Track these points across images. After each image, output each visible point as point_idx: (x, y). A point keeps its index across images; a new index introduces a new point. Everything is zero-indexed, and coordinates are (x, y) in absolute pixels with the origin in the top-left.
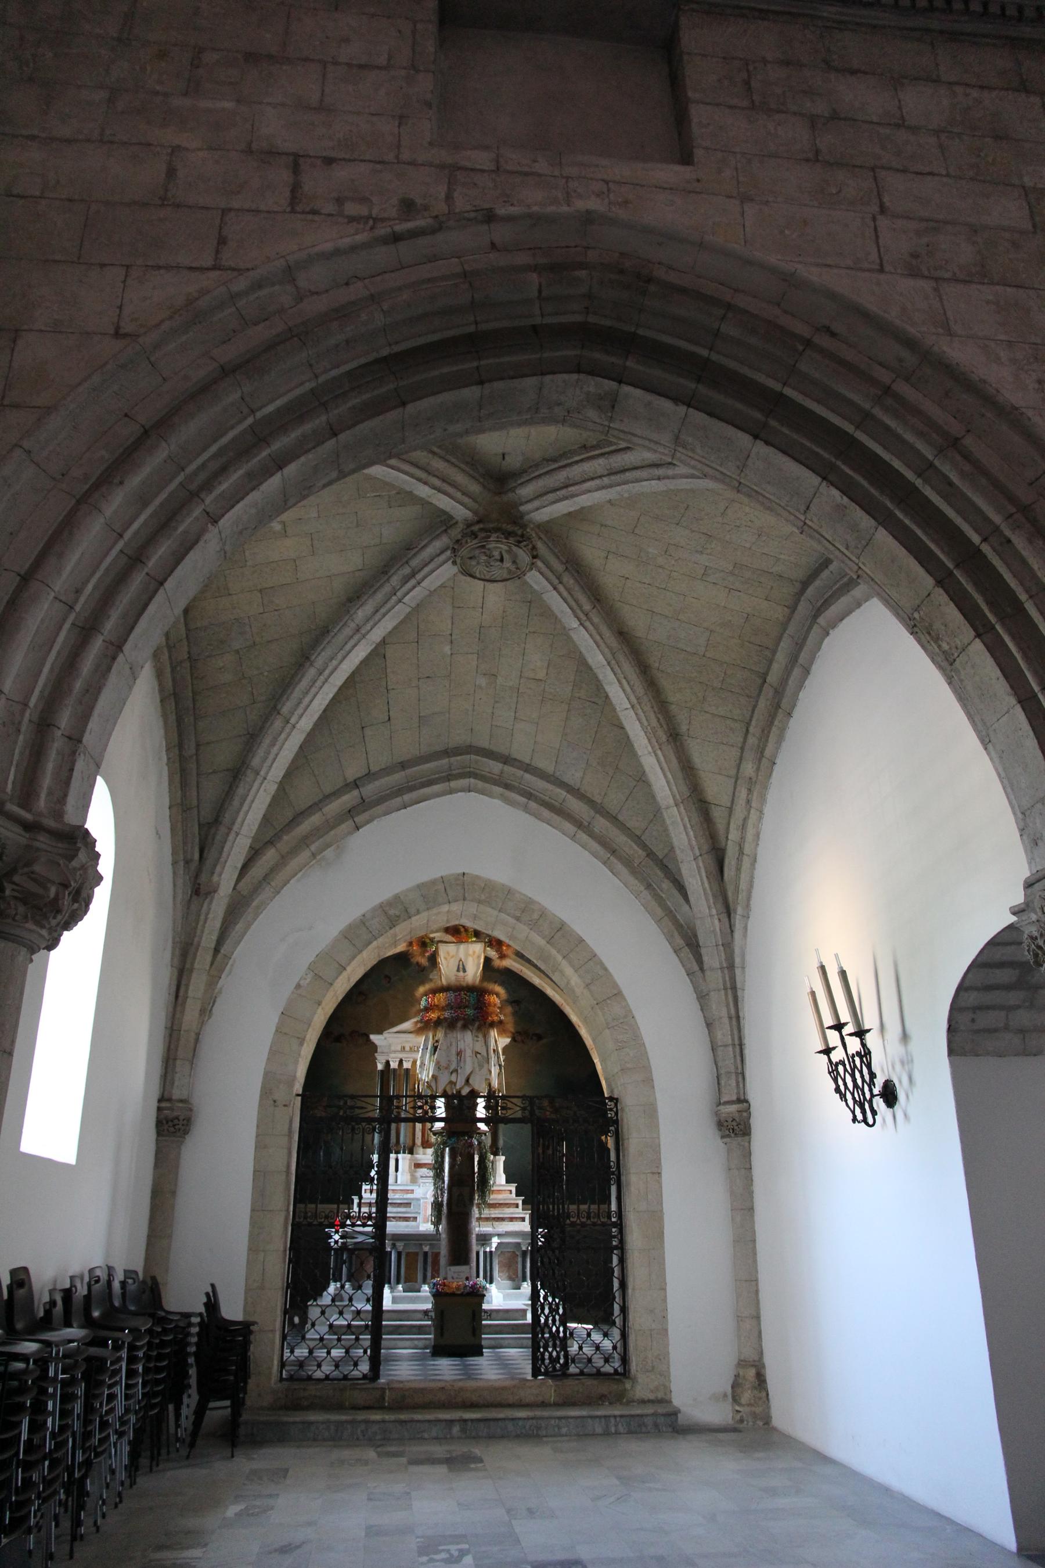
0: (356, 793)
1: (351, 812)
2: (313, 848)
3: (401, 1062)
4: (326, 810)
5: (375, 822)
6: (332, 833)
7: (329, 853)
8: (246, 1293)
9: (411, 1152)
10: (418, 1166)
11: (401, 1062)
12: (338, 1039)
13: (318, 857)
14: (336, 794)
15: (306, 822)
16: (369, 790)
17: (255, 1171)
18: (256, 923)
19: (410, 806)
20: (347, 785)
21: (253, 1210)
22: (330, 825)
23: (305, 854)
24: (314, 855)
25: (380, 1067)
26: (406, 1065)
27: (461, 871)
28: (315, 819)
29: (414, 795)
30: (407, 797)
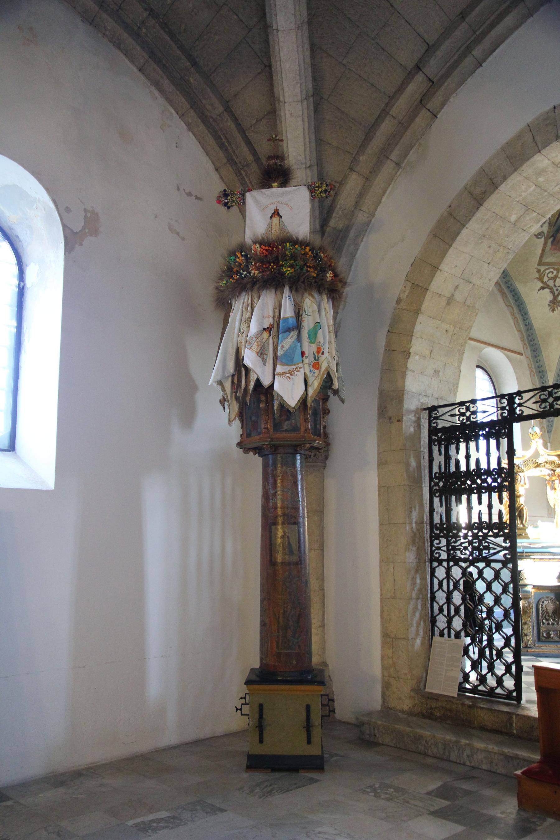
0: (420, 77)
1: (422, 102)
2: (394, 156)
4: (393, 111)
5: (452, 100)
6: (409, 132)
7: (412, 156)
8: (381, 602)
13: (403, 165)
14: (401, 89)
15: (378, 134)
16: (433, 67)
17: (380, 487)
18: (359, 252)
19: (484, 60)
20: (409, 73)
21: (381, 524)
22: (404, 125)
23: (388, 166)
24: (398, 165)
27: (552, 106)
28: (386, 127)
29: (487, 43)
30: (477, 52)
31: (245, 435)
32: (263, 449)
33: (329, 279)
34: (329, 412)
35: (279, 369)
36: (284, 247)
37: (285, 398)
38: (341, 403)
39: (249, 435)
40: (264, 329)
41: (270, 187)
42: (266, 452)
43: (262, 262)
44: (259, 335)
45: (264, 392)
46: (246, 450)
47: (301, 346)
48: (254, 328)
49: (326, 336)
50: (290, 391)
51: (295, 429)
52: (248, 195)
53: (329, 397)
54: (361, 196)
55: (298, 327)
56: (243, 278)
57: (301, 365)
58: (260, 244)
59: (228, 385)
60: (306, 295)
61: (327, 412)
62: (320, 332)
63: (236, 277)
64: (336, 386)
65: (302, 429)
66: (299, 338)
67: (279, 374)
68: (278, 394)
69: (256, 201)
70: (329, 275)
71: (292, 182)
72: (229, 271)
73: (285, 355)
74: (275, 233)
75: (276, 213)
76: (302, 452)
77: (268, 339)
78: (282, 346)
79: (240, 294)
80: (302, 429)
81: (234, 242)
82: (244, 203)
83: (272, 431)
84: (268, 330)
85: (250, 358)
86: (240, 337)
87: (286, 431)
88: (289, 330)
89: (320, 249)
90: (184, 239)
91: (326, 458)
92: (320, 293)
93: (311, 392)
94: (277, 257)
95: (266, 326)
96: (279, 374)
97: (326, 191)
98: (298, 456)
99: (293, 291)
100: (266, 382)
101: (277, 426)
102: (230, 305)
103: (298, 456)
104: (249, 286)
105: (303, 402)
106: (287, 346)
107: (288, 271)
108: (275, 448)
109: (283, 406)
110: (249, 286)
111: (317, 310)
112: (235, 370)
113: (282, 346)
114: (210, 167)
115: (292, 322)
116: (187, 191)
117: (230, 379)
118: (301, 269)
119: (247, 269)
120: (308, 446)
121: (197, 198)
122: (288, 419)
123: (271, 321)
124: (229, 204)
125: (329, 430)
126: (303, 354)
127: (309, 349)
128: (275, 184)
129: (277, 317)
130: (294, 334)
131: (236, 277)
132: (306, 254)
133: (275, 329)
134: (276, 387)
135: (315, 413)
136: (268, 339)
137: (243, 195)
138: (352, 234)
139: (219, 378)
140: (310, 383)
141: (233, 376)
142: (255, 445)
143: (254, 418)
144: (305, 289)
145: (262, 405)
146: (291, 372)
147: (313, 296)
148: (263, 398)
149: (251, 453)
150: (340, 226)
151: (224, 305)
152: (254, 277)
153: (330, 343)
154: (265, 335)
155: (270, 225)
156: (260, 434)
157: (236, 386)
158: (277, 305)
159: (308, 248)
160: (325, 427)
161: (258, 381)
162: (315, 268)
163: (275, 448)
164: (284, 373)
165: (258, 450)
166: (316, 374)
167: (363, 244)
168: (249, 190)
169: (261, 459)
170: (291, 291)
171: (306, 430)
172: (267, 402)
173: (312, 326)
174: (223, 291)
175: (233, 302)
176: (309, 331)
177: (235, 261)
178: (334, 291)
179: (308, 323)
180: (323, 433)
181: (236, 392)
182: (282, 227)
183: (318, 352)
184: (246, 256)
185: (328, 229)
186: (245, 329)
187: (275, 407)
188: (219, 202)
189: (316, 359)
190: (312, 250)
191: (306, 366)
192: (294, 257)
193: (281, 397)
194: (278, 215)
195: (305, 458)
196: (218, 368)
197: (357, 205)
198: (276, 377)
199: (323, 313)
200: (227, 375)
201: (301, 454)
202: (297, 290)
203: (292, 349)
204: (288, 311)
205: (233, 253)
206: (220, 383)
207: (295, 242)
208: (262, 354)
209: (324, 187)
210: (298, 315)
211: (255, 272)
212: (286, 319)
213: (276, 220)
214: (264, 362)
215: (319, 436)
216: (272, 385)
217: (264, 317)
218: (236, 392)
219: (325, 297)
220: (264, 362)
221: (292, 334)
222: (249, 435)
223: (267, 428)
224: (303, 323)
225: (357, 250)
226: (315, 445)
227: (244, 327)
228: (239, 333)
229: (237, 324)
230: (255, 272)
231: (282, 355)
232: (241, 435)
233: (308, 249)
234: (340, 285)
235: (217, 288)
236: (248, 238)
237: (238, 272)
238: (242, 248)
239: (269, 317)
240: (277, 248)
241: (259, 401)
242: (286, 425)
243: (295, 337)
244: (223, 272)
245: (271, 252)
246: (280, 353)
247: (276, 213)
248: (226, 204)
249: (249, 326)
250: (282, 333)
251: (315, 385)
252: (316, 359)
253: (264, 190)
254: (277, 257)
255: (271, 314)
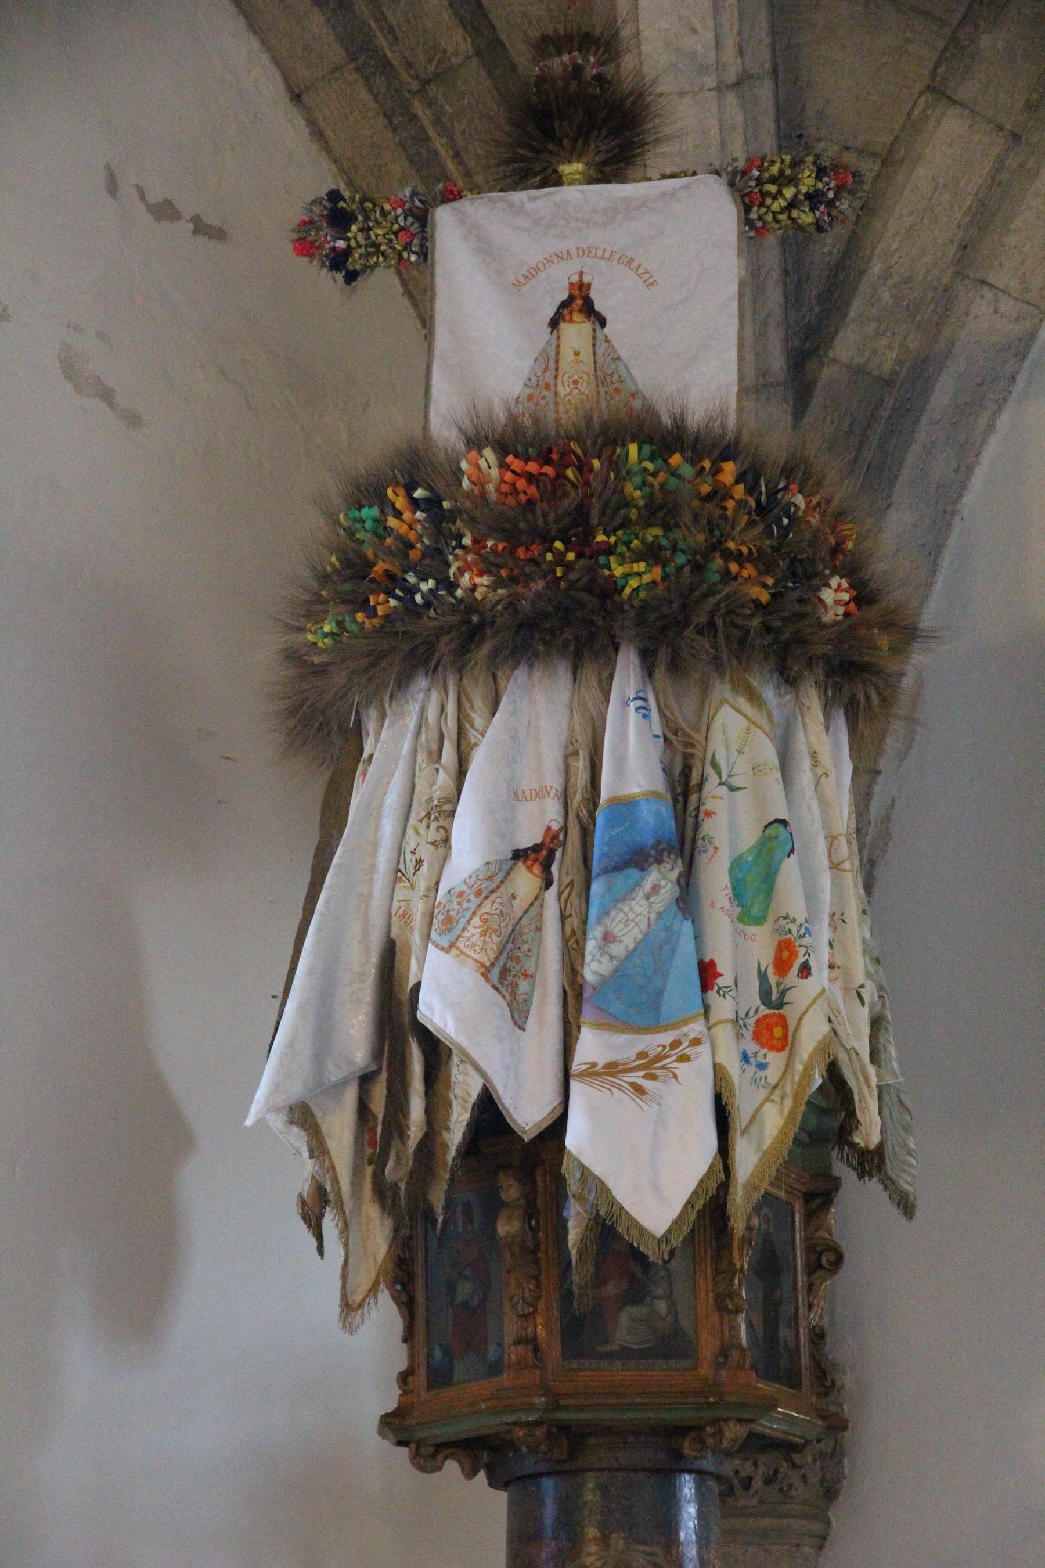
18: (978, 481)
31: (422, 1376)
32: (512, 1445)
33: (833, 614)
34: (838, 1260)
35: (591, 1046)
36: (615, 464)
37: (623, 1193)
38: (896, 1213)
39: (440, 1377)
40: (518, 855)
41: (553, 180)
42: (530, 1465)
43: (511, 535)
44: (493, 881)
45: (515, 1160)
46: (428, 1454)
47: (698, 938)
48: (470, 849)
49: (817, 888)
50: (644, 1156)
51: (672, 1345)
52: (444, 216)
53: (836, 1183)
54: (986, 217)
55: (684, 844)
56: (413, 611)
57: (696, 1028)
58: (503, 448)
59: (340, 1126)
60: (722, 689)
61: (826, 1259)
62: (790, 870)
63: (386, 604)
64: (870, 1131)
65: (708, 1346)
66: (687, 898)
67: (591, 1073)
68: (585, 1173)
69: (487, 251)
70: (834, 596)
71: (657, 158)
72: (352, 577)
73: (618, 978)
74: (573, 396)
75: (579, 303)
76: (708, 1464)
77: (538, 898)
78: (608, 938)
79: (403, 682)
80: (708, 1346)
81: (380, 434)
82: (425, 254)
83: (553, 1351)
84: (539, 856)
85: (447, 994)
86: (401, 892)
87: (627, 1354)
88: (638, 859)
89: (788, 471)
90: (133, 420)
91: (830, 1492)
92: (790, 680)
93: (746, 1159)
94: (581, 513)
95: (529, 837)
96: (591, 1073)
97: (814, 199)
98: (687, 1486)
99: (660, 672)
100: (527, 1114)
101: (580, 1331)
102: (358, 733)
103: (687, 1486)
104: (445, 647)
105: (711, 1209)
106: (628, 938)
107: (633, 576)
108: (570, 1443)
109: (610, 1230)
110: (445, 647)
111: (776, 764)
112: (377, 1054)
113: (608, 938)
114: (266, 84)
115: (655, 818)
116: (155, 196)
117: (351, 1096)
118: (698, 568)
119: (435, 563)
120: (733, 1432)
121: (200, 227)
122: (636, 1294)
123: (551, 813)
124: (355, 262)
125: (837, 1351)
126: (707, 973)
127: (740, 951)
128: (572, 168)
129: (582, 801)
130: (662, 879)
131: (386, 604)
132: (719, 495)
133: (569, 854)
134: (575, 1138)
135: (770, 1266)
136: (538, 898)
137: (423, 219)
138: (942, 395)
139: (296, 1090)
140: (741, 1116)
141: (365, 1080)
142: (465, 1428)
143: (465, 1290)
144: (717, 664)
145: (507, 1227)
146: (650, 1064)
147: (754, 697)
148: (511, 1190)
149: (452, 1467)
150: (887, 358)
151: (325, 735)
152: (470, 606)
153: (838, 919)
154: (525, 881)
155: (551, 361)
156: (495, 1369)
157: (379, 1130)
158: (583, 739)
159: (729, 468)
160: (818, 1337)
161: (488, 1110)
162: (764, 562)
163: (570, 1443)
164: (613, 1069)
165: (485, 1453)
166: (773, 1074)
167: (993, 443)
168: (451, 196)
169: (502, 1497)
170: (649, 671)
171: (724, 1353)
172: (530, 1212)
173: (749, 837)
174: (321, 671)
175: (370, 724)
176: (736, 864)
177: (381, 530)
178: (854, 668)
179: (730, 826)
180: (808, 1368)
181: (379, 1162)
182: (606, 372)
183: (782, 966)
184: (432, 504)
185: (827, 374)
186: (426, 852)
187: (573, 1236)
188: (305, 247)
189: (773, 999)
190: (749, 477)
191: (724, 1035)
192: (661, 510)
193: (603, 1189)
194: (589, 309)
195: (724, 1494)
196: (291, 1045)
197: (967, 257)
198: (576, 1087)
199: (805, 777)
200: (334, 1074)
201: (701, 1475)
202: (676, 667)
203: (655, 950)
204: (633, 767)
205: (369, 492)
206: (302, 1116)
207: (668, 439)
208: (506, 973)
209: (808, 182)
210: (684, 784)
211: (474, 583)
212: (625, 805)
213: (576, 333)
214: (519, 1014)
215: (792, 1379)
216: (558, 1127)
217: (516, 796)
218: (379, 1162)
219: (813, 699)
220: (519, 1014)
221: (653, 876)
222: (440, 1377)
223: (532, 1342)
224: (708, 827)
225: (965, 470)
226: (771, 1426)
227: (420, 840)
228: (398, 874)
229: (388, 827)
230: (474, 583)
231: (604, 981)
232: (404, 1378)
233: (729, 468)
234: (884, 642)
235: (293, 656)
236: (445, 421)
237: (392, 582)
238: (416, 467)
239: (540, 794)
240: (582, 467)
241: (493, 1206)
242: (626, 1327)
243: (669, 890)
244: (324, 579)
245: (555, 488)
246: (594, 968)
247: (579, 303)
248: (338, 261)
249: (446, 841)
250: (606, 871)
251: (768, 1125)
252: (773, 999)
253: (518, 196)
254: (581, 513)
255: (554, 780)
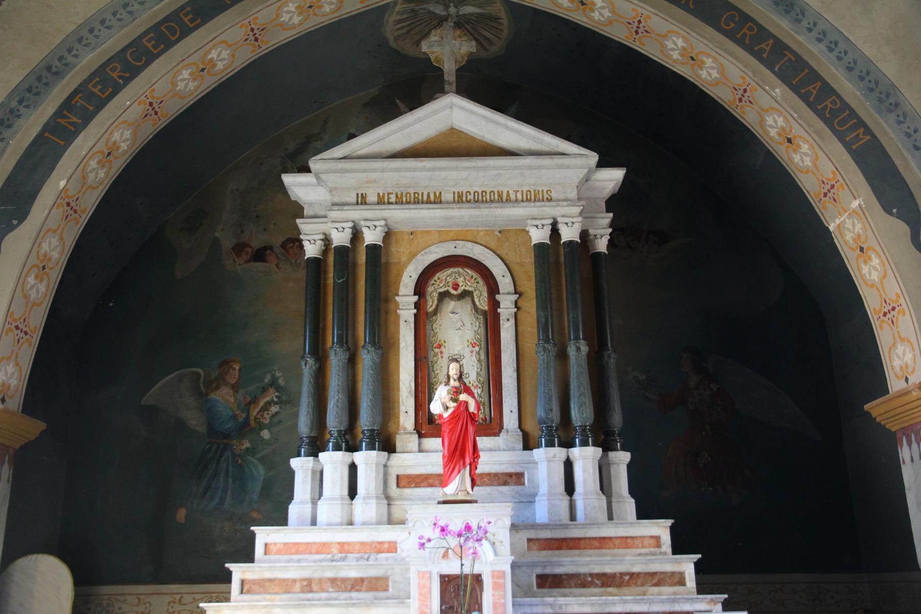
3: (356, 235)
9: (389, 447)
10: (405, 481)
11: (356, 235)
12: (260, 255)
25: (311, 250)
26: (371, 237)
